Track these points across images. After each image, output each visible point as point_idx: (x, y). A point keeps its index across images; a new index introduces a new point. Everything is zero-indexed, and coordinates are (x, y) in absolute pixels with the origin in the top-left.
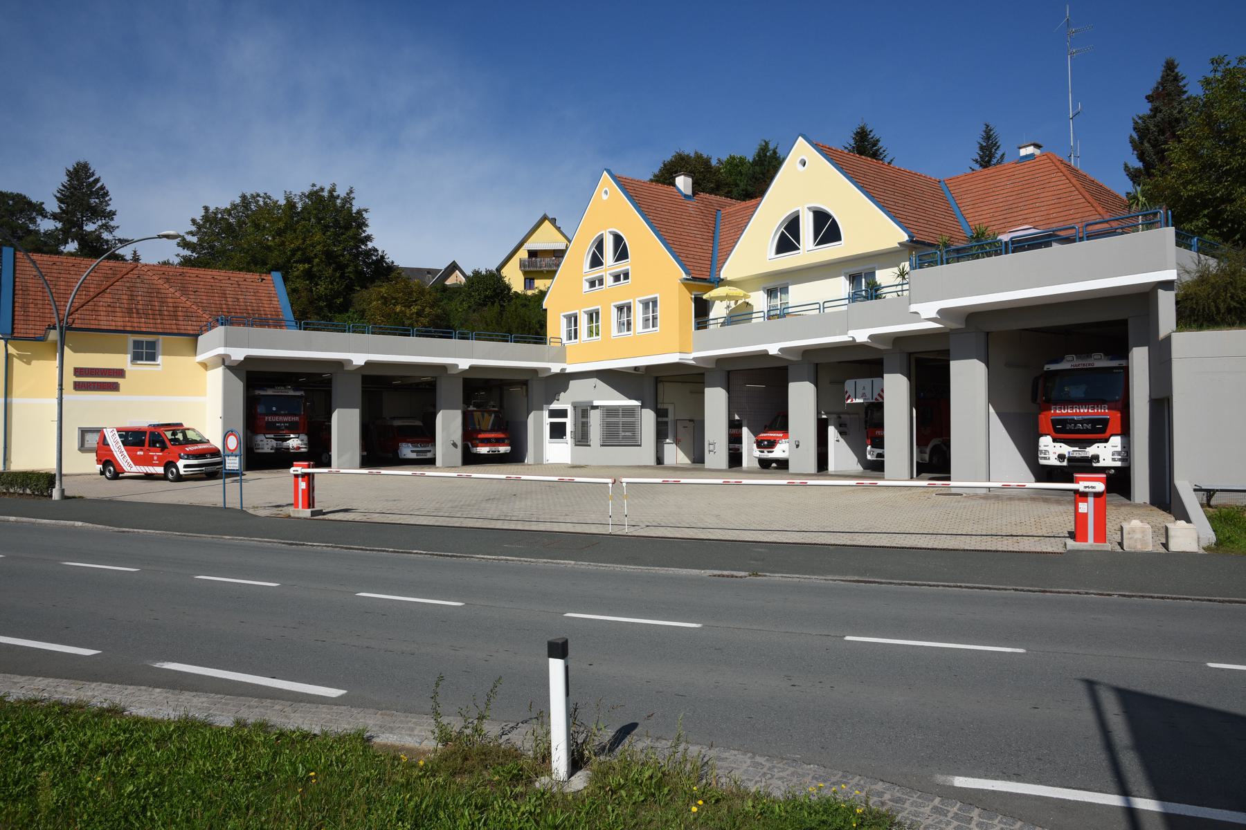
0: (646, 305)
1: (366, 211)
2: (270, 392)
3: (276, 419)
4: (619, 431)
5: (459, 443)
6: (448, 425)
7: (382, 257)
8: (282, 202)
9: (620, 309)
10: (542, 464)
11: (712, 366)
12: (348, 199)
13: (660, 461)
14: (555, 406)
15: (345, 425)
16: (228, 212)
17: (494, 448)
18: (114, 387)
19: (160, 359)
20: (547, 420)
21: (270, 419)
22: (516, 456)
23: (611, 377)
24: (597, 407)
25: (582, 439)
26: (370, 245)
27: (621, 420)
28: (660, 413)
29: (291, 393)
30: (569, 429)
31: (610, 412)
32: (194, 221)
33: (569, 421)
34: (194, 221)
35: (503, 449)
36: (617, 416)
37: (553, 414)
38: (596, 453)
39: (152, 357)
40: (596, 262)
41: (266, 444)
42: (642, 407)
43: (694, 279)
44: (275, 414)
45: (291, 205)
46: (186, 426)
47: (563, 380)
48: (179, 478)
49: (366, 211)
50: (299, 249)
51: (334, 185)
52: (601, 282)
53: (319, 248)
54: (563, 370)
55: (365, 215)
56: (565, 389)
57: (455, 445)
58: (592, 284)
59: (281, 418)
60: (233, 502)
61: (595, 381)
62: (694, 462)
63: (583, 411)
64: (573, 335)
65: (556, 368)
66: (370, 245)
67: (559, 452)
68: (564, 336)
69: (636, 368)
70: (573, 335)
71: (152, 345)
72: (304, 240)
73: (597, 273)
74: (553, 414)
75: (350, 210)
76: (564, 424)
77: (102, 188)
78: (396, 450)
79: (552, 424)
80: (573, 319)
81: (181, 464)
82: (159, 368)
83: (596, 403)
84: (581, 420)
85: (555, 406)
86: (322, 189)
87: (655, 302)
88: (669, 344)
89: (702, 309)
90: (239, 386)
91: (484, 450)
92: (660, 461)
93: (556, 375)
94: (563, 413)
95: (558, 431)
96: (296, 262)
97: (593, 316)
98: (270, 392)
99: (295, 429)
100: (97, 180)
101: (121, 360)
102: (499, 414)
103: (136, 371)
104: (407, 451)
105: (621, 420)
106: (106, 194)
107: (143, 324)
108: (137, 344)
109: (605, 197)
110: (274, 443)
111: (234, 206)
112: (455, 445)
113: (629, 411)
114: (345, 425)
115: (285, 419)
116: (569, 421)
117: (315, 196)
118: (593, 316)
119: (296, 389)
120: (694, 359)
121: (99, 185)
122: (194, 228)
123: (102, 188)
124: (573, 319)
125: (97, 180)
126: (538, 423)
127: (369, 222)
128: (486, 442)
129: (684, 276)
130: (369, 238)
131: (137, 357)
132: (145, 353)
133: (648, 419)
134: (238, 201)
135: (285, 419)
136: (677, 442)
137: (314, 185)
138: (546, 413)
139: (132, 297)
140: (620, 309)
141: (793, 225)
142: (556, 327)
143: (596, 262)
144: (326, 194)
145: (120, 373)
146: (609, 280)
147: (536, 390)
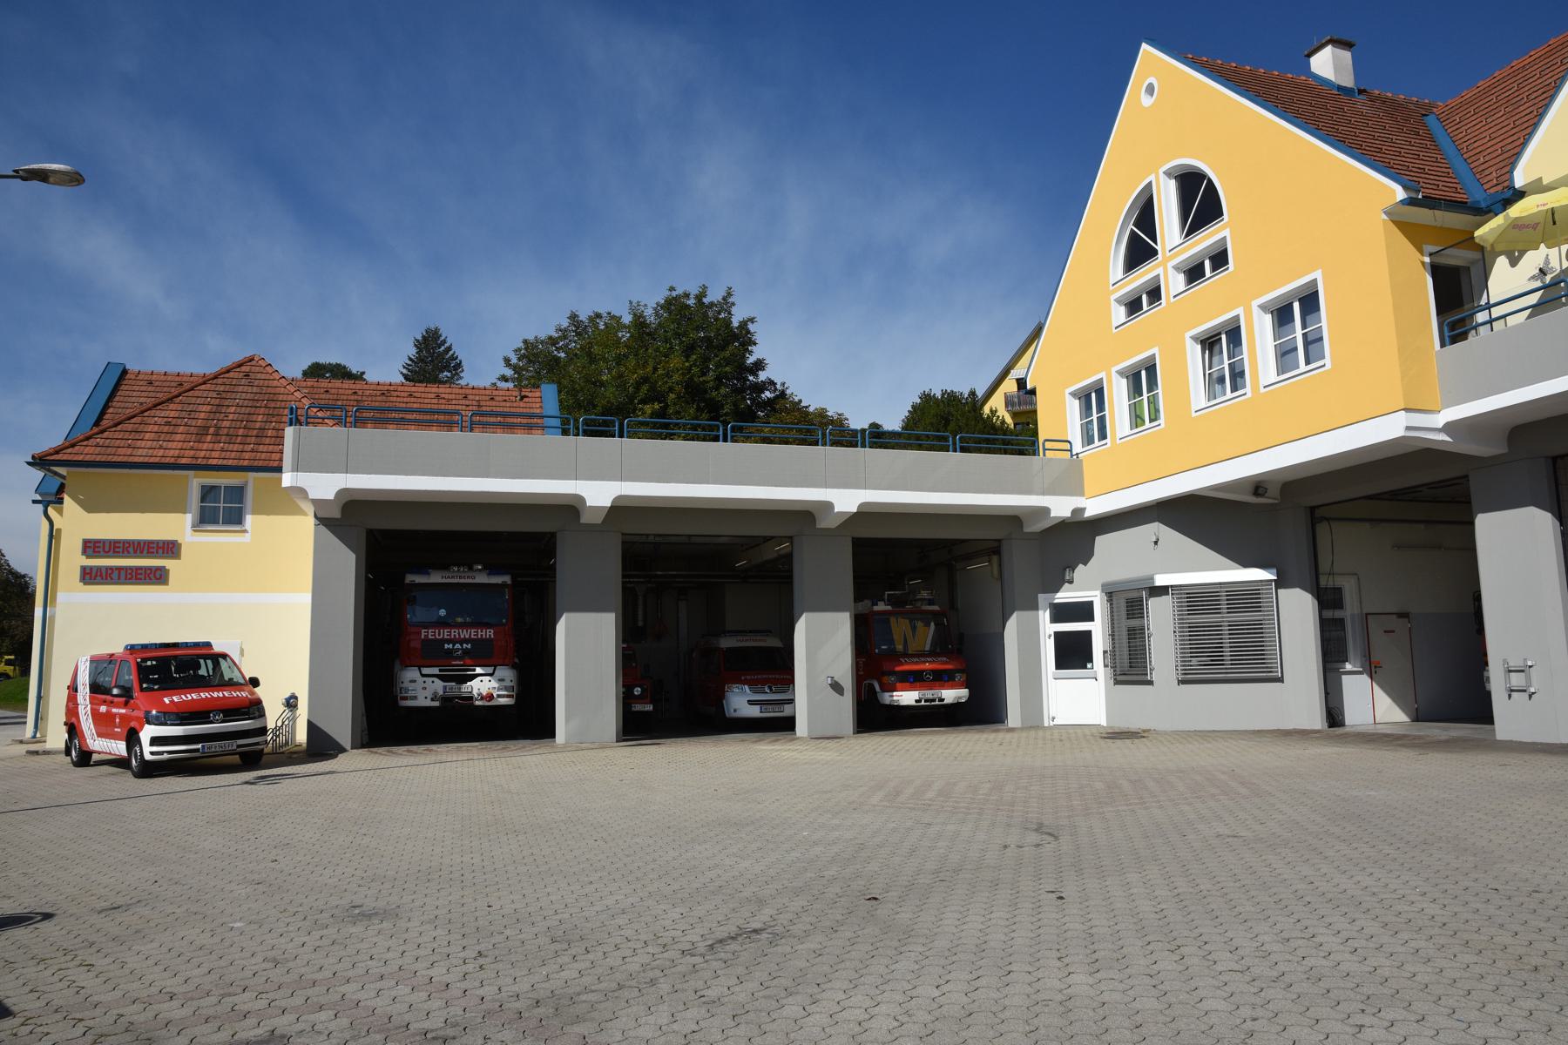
0: (1282, 315)
1: (752, 320)
2: (436, 578)
3: (444, 633)
4: (1226, 645)
5: (847, 683)
6: (822, 644)
7: (783, 394)
8: (627, 319)
9: (1209, 343)
10: (1039, 727)
11: (1501, 449)
12: (726, 304)
13: (1334, 717)
14: (1065, 596)
15: (585, 646)
16: (552, 341)
17: (929, 694)
18: (158, 577)
19: (249, 520)
20: (1048, 628)
21: (431, 634)
22: (983, 709)
23: (1193, 515)
24: (1163, 591)
25: (1131, 667)
26: (763, 376)
27: (1225, 618)
28: (1328, 600)
29: (482, 579)
30: (1099, 645)
31: (1196, 600)
32: (507, 361)
33: (1098, 629)
34: (507, 361)
35: (950, 695)
36: (1216, 610)
37: (1062, 613)
38: (1172, 702)
39: (235, 518)
40: (1140, 252)
41: (422, 688)
42: (1280, 583)
43: (1430, 202)
44: (442, 624)
45: (639, 322)
46: (217, 649)
47: (1078, 537)
48: (149, 770)
49: (752, 320)
50: (645, 380)
51: (705, 287)
52: (1155, 294)
53: (676, 377)
54: (1078, 511)
55: (751, 327)
56: (1086, 555)
57: (837, 687)
58: (1133, 306)
59: (455, 633)
61: (1155, 529)
62: (1417, 717)
63: (1131, 602)
64: (1095, 430)
65: (1061, 507)
66: (763, 376)
67: (1077, 700)
68: (1075, 436)
70: (1095, 430)
71: (237, 493)
72: (655, 369)
73: (1144, 275)
74: (1062, 613)
75: (727, 323)
76: (1088, 634)
78: (719, 699)
79: (1059, 636)
80: (1093, 397)
81: (148, 732)
82: (247, 538)
83: (1161, 580)
84: (1125, 624)
85: (1065, 596)
86: (687, 295)
87: (1310, 301)
88: (1373, 396)
89: (1456, 296)
90: (347, 562)
91: (907, 697)
92: (1334, 717)
94: (1083, 611)
95: (1073, 653)
96: (644, 402)
97: (1142, 377)
98: (436, 578)
99: (485, 655)
100: (449, 349)
101: (176, 525)
102: (937, 614)
103: (203, 546)
104: (741, 702)
106: (459, 365)
107: (209, 451)
108: (208, 492)
109: (1147, 101)
110: (439, 685)
111: (564, 333)
112: (837, 687)
114: (585, 646)
115: (465, 634)
116: (1098, 629)
117: (674, 306)
118: (1142, 377)
119: (492, 569)
120: (1449, 428)
122: (509, 372)
123: (454, 358)
124: (1093, 397)
125: (449, 349)
126: (1029, 636)
127: (757, 337)
128: (914, 680)
129: (1400, 194)
130: (760, 365)
132: (221, 510)
133: (1297, 614)
134: (565, 323)
135: (465, 634)
136: (1371, 669)
137: (672, 289)
138: (1045, 616)
140: (1209, 343)
142: (1060, 419)
143: (1140, 252)
144: (691, 302)
145: (170, 549)
146: (1174, 283)
147: (1018, 561)
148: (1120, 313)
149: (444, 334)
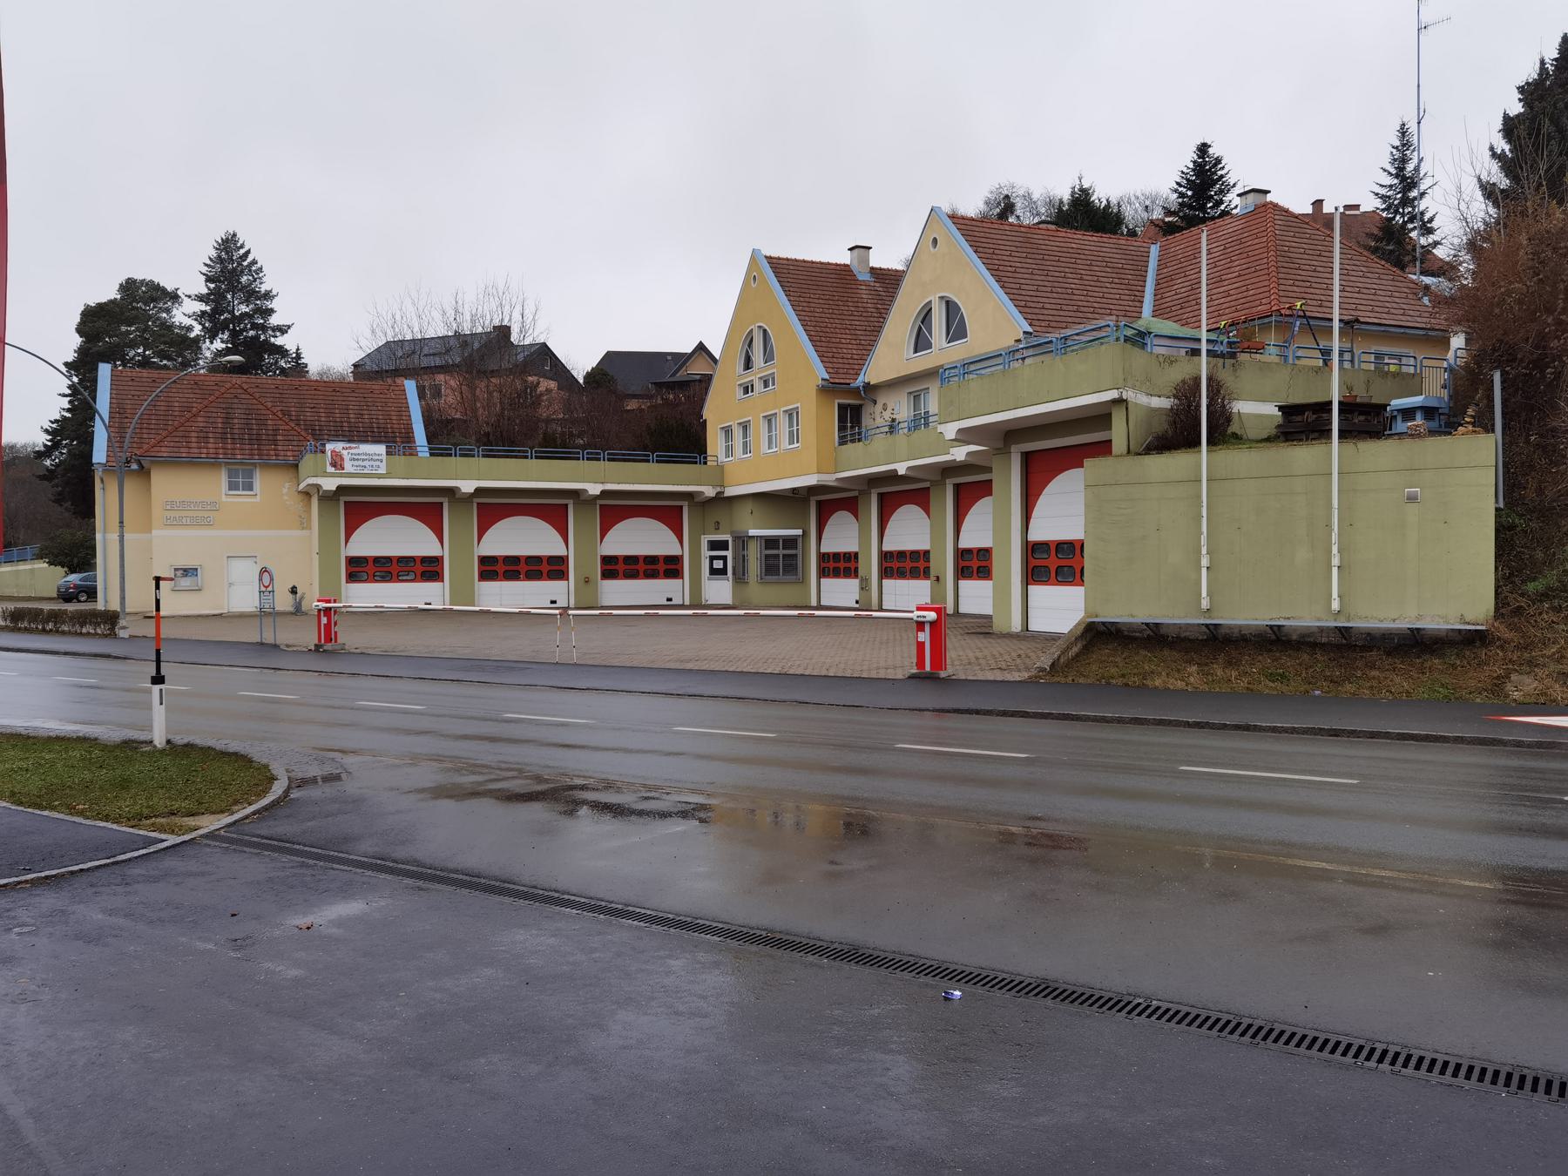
25: (740, 578)
27: (781, 552)
31: (770, 542)
58: (746, 391)
60: (269, 638)
64: (729, 451)
69: (794, 490)
70: (729, 451)
77: (254, 262)
83: (752, 532)
93: (711, 500)
94: (723, 545)
97: (745, 427)
100: (248, 252)
105: (781, 552)
113: (790, 542)
121: (250, 259)
123: (254, 262)
124: (728, 431)
131: (233, 486)
139: (227, 419)
141: (926, 316)
143: (748, 364)
146: (758, 386)
148: (740, 393)
149: (241, 238)
